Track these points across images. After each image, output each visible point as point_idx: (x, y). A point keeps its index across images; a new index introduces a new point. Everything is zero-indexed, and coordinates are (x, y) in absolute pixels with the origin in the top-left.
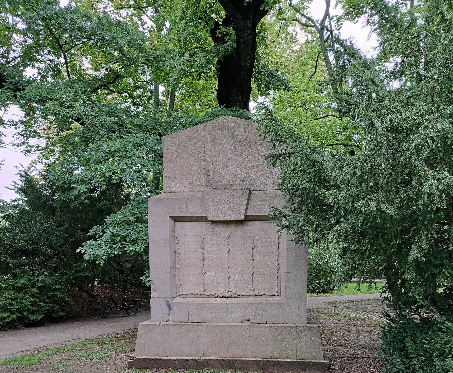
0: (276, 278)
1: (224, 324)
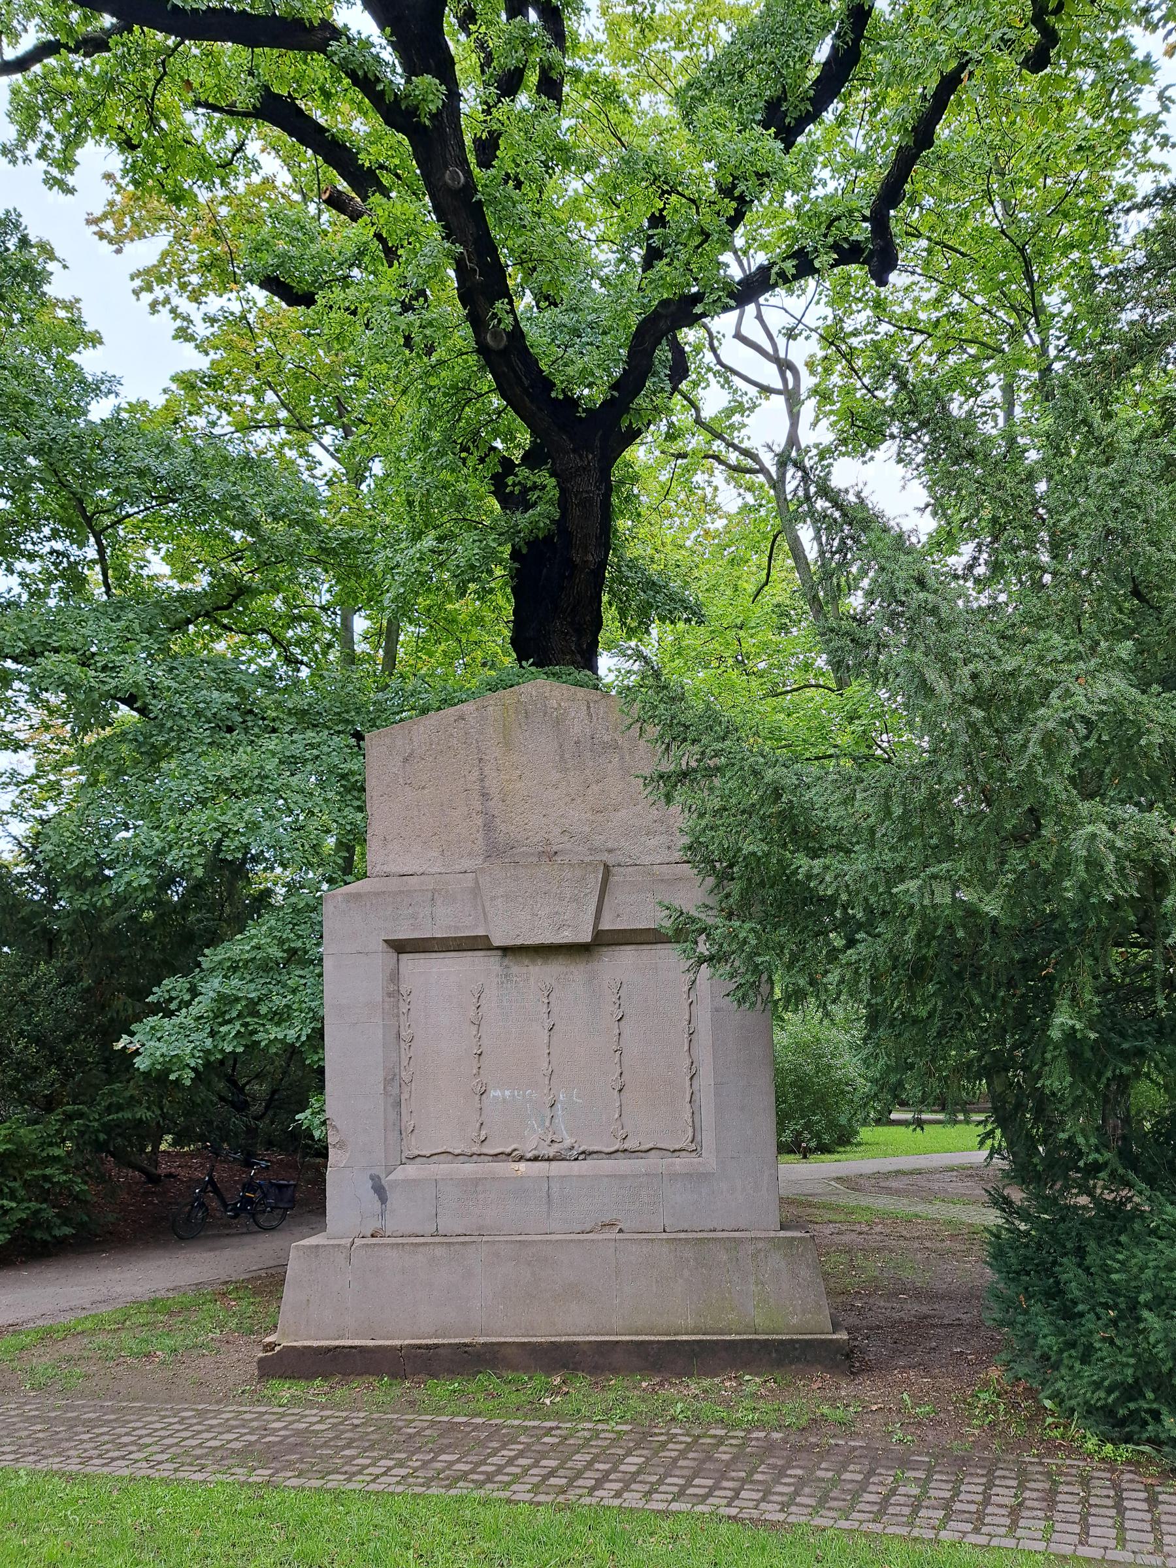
1: (539, 1237)
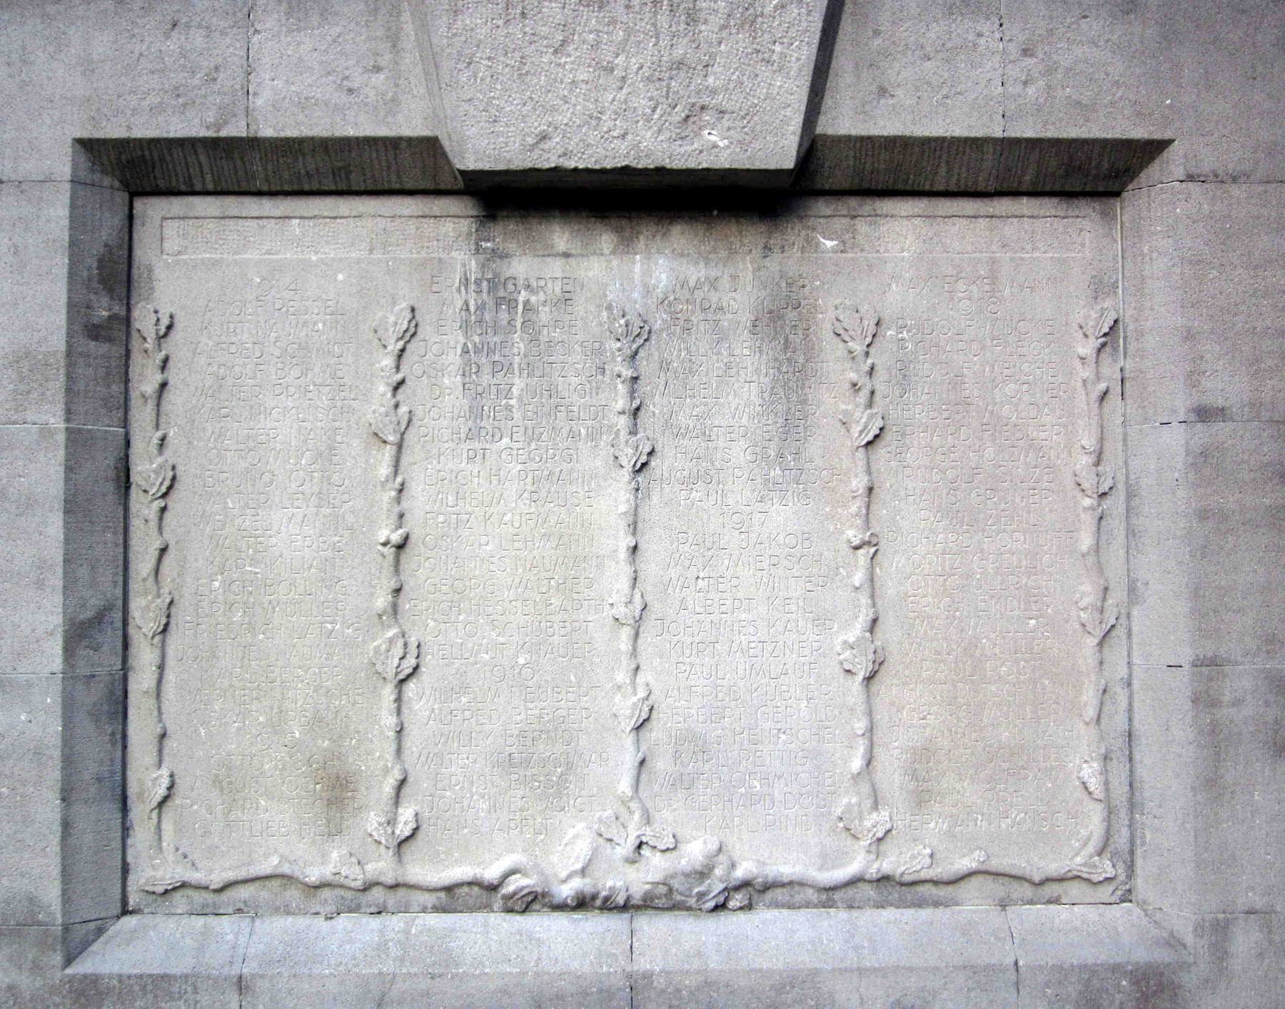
0: (1091, 712)
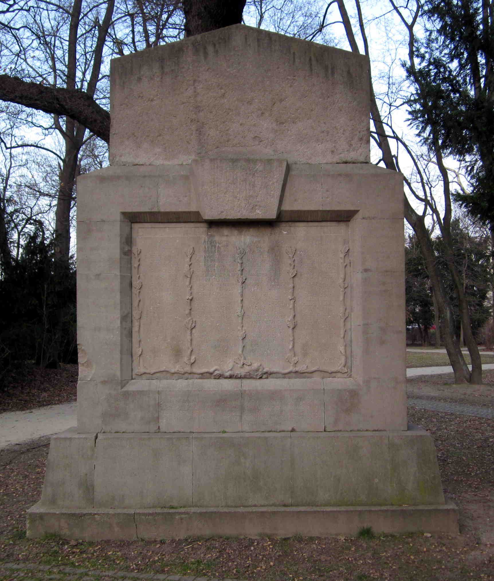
0: (342, 336)
